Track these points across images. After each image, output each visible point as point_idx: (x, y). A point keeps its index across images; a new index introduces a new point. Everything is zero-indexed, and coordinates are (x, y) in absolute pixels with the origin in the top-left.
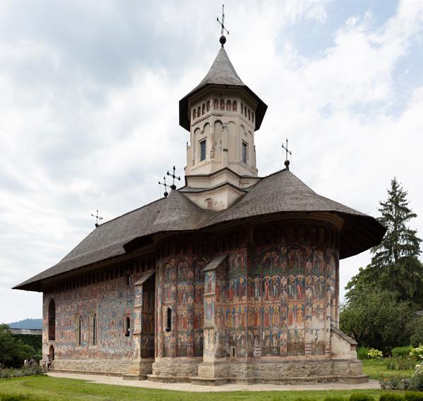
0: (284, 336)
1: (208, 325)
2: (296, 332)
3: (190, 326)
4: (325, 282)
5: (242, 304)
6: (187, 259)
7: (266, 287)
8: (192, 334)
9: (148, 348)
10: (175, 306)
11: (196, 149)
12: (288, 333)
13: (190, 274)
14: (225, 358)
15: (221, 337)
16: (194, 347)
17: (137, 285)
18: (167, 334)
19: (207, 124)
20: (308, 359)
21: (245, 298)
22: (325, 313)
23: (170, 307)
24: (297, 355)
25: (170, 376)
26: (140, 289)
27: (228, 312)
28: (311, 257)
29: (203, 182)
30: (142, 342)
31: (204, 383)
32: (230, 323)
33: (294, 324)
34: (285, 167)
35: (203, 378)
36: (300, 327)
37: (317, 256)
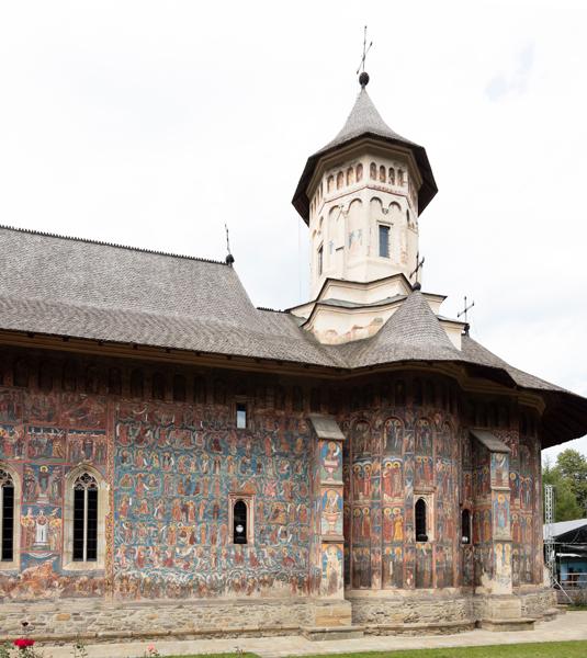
1: (499, 537)
5: (514, 509)
25: (443, 622)
35: (501, 621)
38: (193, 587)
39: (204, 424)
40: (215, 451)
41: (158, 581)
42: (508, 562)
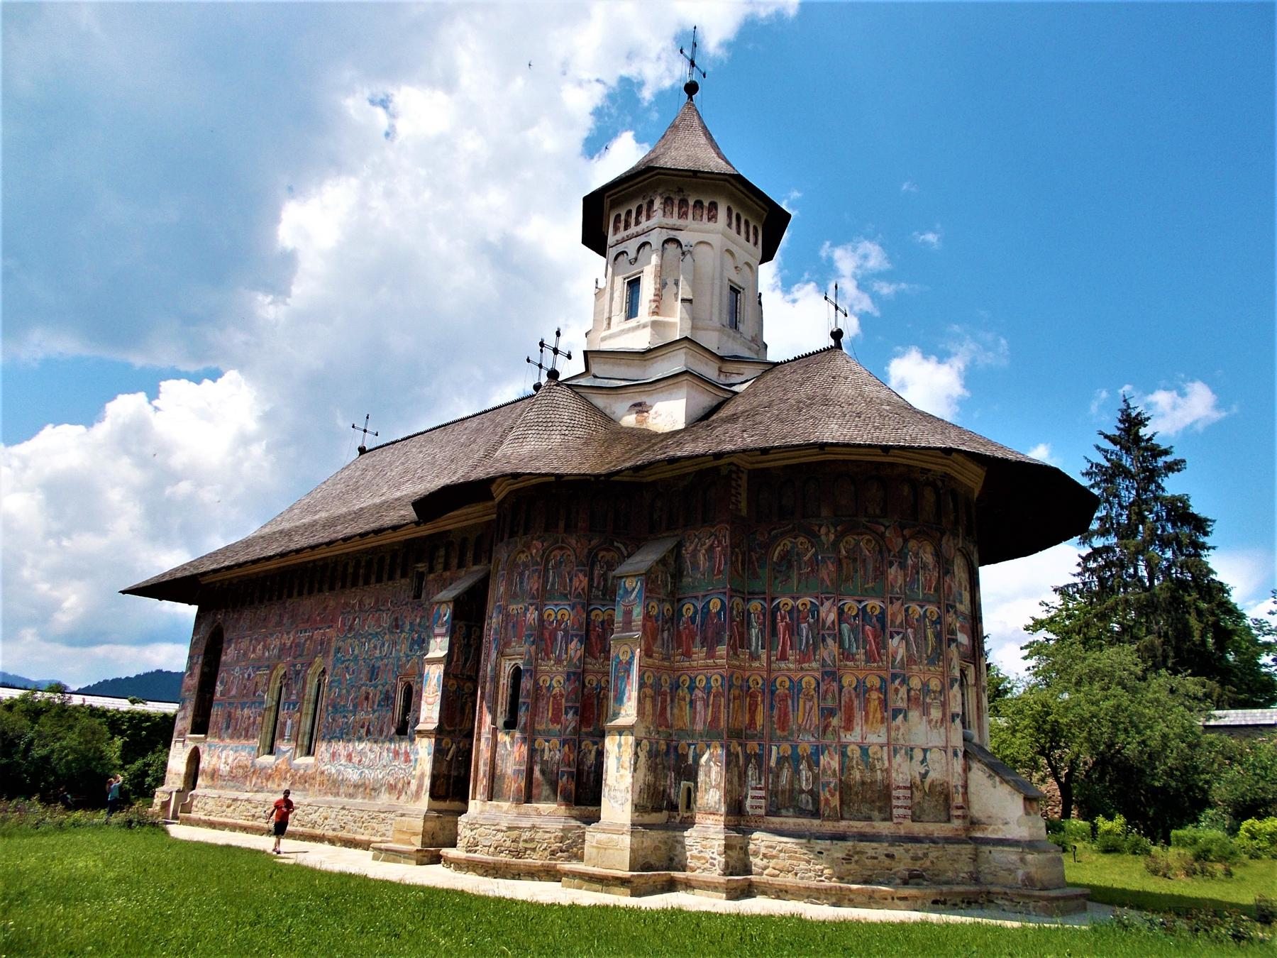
0: (831, 762)
2: (864, 750)
3: (570, 719)
4: (939, 621)
5: (716, 666)
6: (574, 542)
7: (781, 626)
8: (573, 742)
9: (454, 773)
10: (533, 661)
11: (617, 294)
12: (843, 754)
13: (581, 582)
14: (665, 813)
15: (652, 754)
16: (578, 776)
17: (441, 603)
18: (503, 738)
19: (644, 244)
20: (902, 832)
21: (722, 650)
22: (944, 705)
23: (520, 662)
24: (869, 819)
25: (504, 858)
26: (447, 612)
27: (676, 686)
28: (902, 556)
29: (629, 366)
30: (439, 753)
31: (598, 887)
32: (681, 716)
33: (857, 729)
34: (832, 342)
36: (876, 738)
37: (916, 555)
38: (361, 786)
39: (391, 602)
40: (394, 630)
41: (341, 778)
42: (627, 764)
